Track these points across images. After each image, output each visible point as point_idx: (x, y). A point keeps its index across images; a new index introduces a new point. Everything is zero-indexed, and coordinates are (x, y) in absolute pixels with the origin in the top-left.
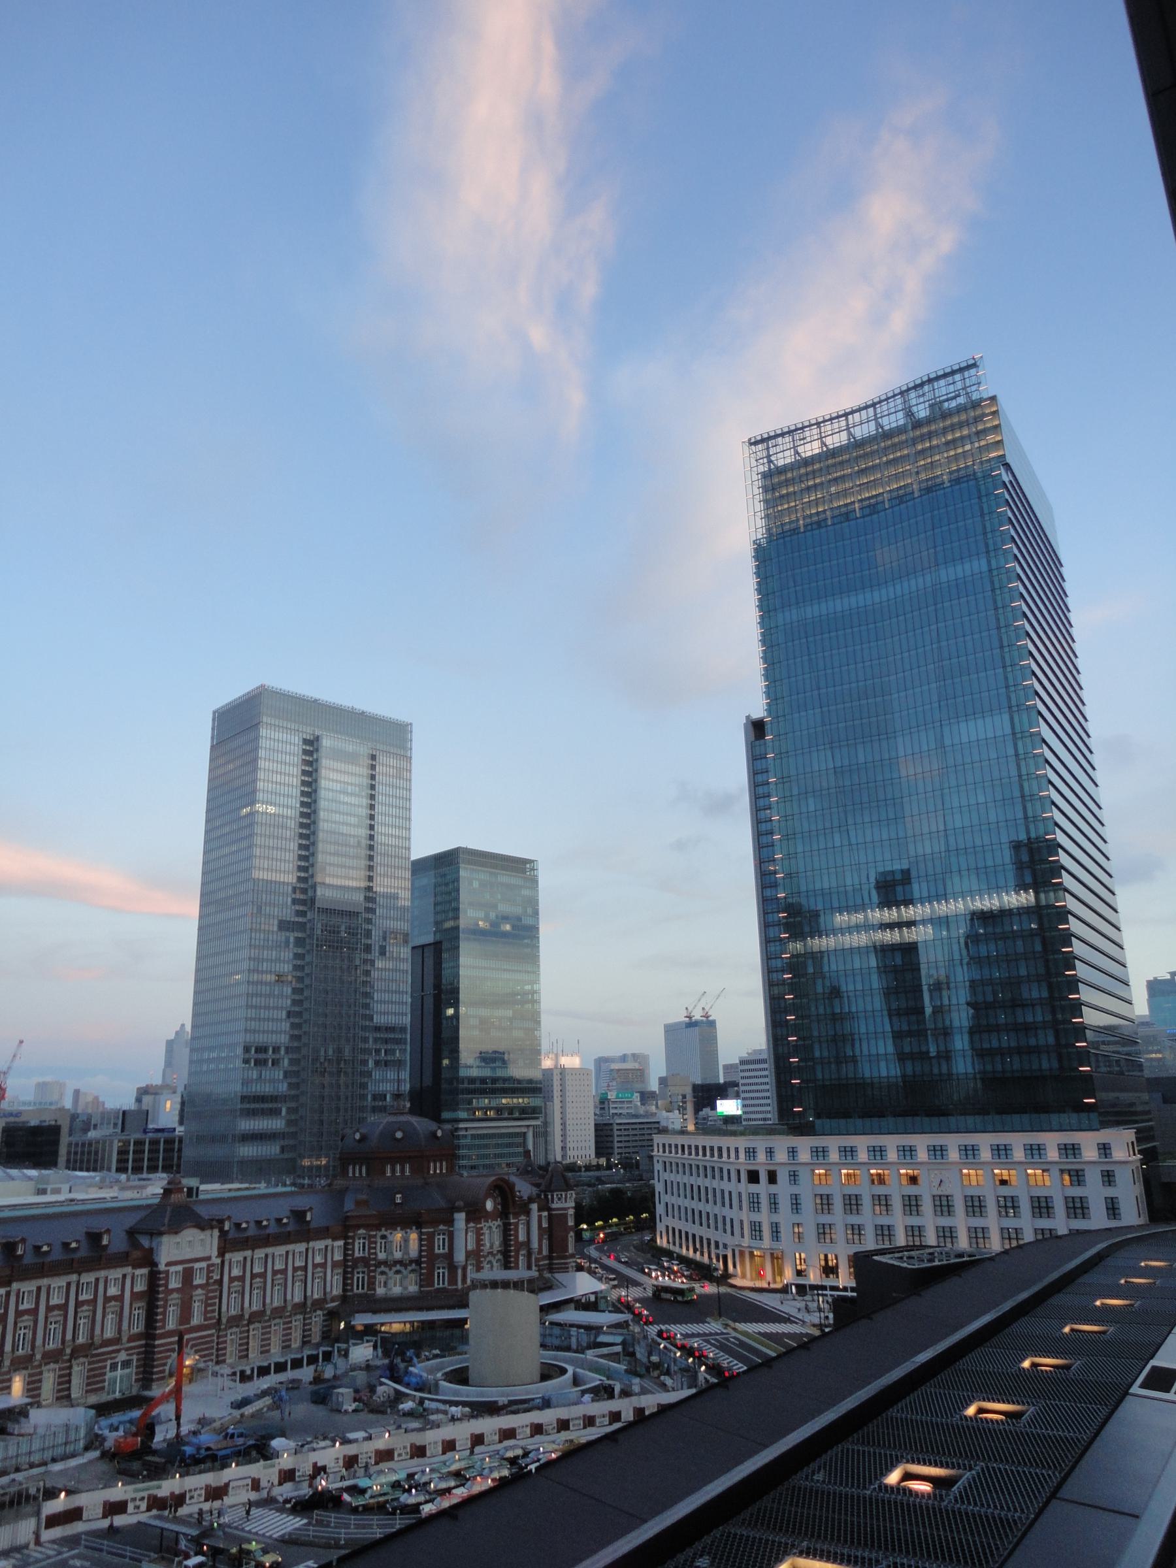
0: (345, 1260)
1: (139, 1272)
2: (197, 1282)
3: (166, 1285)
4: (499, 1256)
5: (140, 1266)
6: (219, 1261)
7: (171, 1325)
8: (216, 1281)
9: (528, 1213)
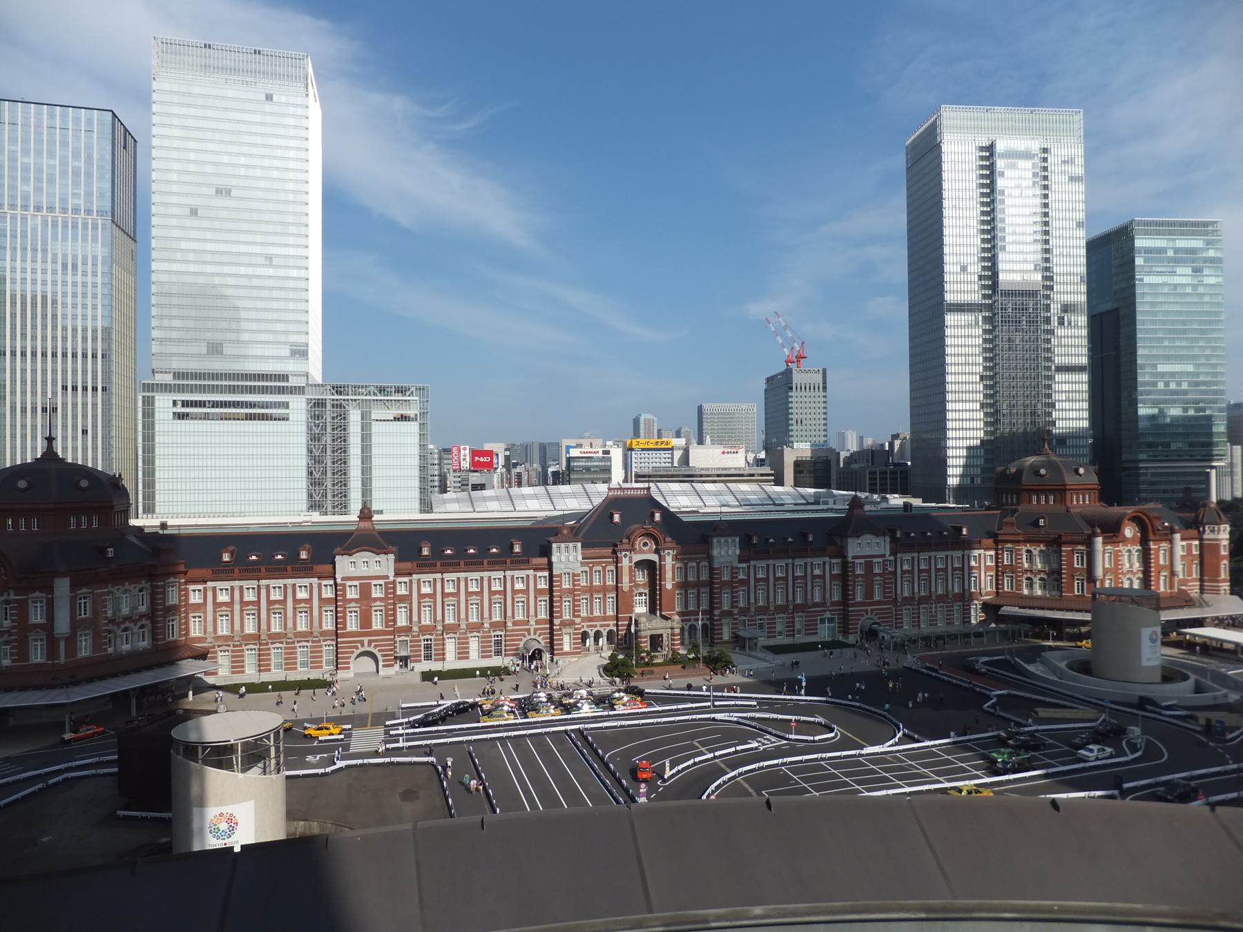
0: (997, 566)
1: (834, 561)
2: (877, 571)
3: (854, 571)
4: (1141, 575)
5: (836, 557)
6: (892, 558)
7: (859, 599)
8: (890, 573)
9: (1171, 541)
